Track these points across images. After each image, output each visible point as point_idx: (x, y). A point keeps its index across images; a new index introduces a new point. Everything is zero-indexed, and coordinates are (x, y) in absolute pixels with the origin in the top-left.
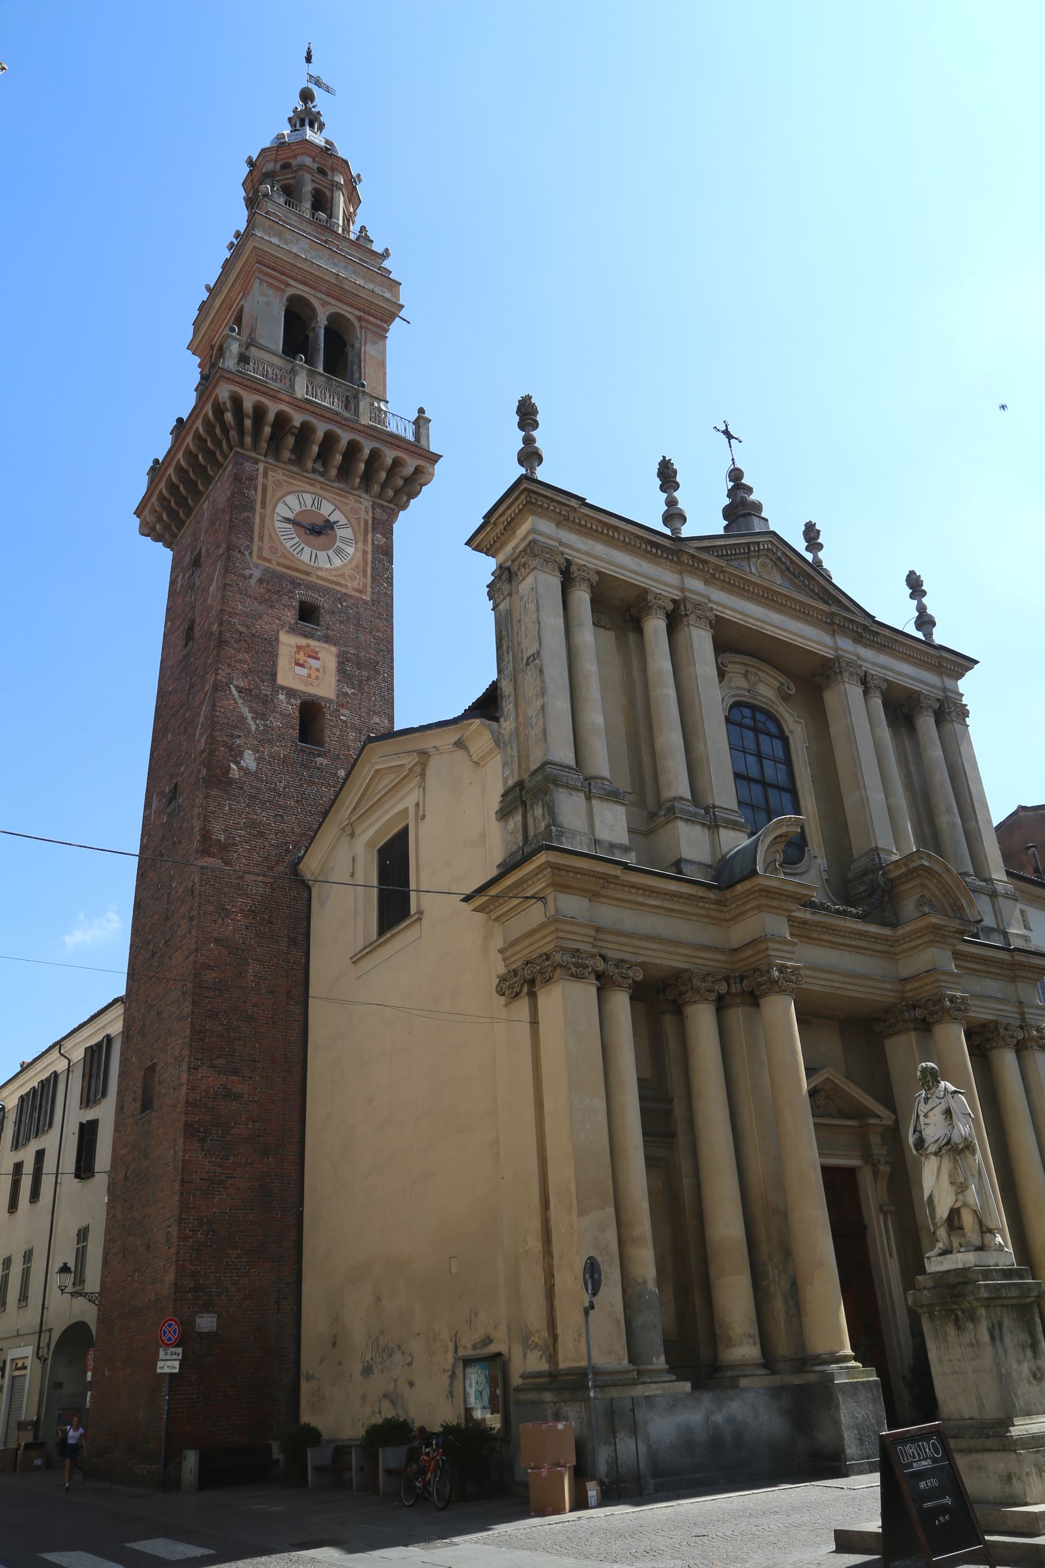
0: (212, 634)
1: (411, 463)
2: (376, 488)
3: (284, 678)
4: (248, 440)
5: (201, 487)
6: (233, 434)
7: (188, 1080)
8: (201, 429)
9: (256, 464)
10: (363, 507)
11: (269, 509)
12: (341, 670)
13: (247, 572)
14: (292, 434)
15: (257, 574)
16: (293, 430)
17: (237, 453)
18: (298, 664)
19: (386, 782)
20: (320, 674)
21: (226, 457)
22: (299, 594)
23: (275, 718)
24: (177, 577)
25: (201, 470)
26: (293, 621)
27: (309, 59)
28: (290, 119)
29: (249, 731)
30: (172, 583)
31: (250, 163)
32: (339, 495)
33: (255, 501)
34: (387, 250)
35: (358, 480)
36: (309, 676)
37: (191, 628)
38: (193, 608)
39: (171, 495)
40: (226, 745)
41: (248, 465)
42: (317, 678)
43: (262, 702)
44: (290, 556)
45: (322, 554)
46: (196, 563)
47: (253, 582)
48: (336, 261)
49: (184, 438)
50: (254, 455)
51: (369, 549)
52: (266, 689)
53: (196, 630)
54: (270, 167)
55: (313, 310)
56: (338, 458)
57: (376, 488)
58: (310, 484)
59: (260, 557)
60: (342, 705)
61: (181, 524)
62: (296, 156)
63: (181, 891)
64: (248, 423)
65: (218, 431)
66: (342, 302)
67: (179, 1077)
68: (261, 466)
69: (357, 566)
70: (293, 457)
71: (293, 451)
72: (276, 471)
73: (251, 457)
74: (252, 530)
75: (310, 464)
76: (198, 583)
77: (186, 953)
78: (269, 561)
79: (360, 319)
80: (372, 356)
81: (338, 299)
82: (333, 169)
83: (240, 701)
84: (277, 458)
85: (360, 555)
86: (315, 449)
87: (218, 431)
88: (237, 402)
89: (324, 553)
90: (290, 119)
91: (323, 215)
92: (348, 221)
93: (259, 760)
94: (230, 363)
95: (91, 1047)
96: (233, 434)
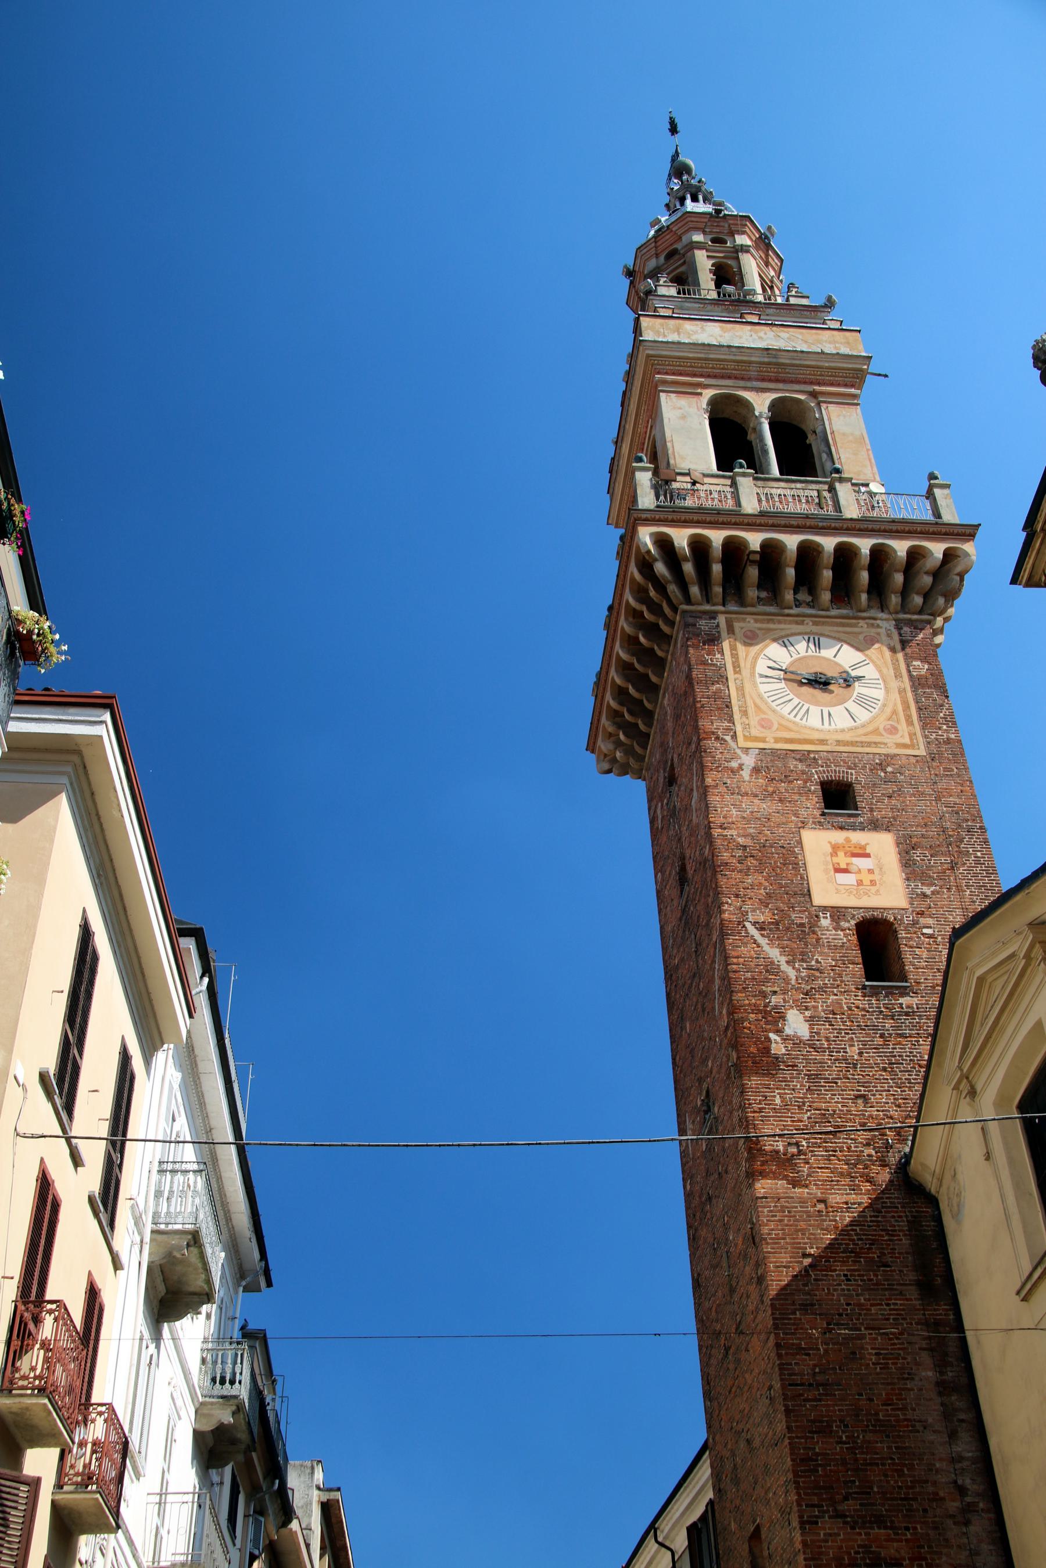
0: (706, 860)
1: (937, 549)
2: (894, 600)
4: (695, 590)
5: (654, 679)
6: (672, 588)
7: (804, 1543)
8: (631, 601)
9: (714, 618)
10: (882, 631)
11: (746, 673)
12: (907, 864)
13: (734, 764)
14: (753, 562)
15: (749, 761)
16: (752, 557)
17: (684, 612)
18: (838, 870)
19: (999, 990)
20: (876, 877)
21: (672, 624)
23: (821, 954)
24: (655, 812)
25: (646, 655)
26: (817, 813)
27: (674, 129)
28: (667, 206)
29: (787, 980)
30: (653, 821)
31: (630, 273)
32: (843, 625)
34: (829, 299)
35: (864, 597)
36: (860, 883)
37: (683, 869)
38: (680, 839)
39: (621, 704)
40: (756, 1010)
41: (703, 624)
42: (873, 883)
44: (791, 725)
45: (838, 711)
46: (671, 780)
47: (746, 774)
48: (762, 334)
49: (617, 622)
50: (707, 607)
51: (907, 684)
53: (688, 867)
54: (652, 264)
55: (748, 406)
56: (827, 575)
57: (894, 600)
58: (797, 623)
59: (746, 738)
60: (921, 914)
61: (644, 739)
62: (680, 238)
63: (740, 1242)
64: (688, 568)
65: (652, 593)
66: (784, 381)
67: (791, 1540)
68: (722, 619)
69: (894, 712)
70: (764, 594)
71: (760, 587)
72: (744, 620)
73: (705, 612)
74: (729, 706)
75: (789, 596)
76: (678, 805)
77: (763, 1337)
79: (814, 395)
80: (844, 434)
81: (777, 380)
82: (732, 234)
83: (763, 942)
84: (742, 602)
85: (896, 696)
86: (791, 572)
87: (652, 593)
88: (664, 544)
89: (841, 708)
90: (667, 206)
91: (730, 289)
92: (771, 288)
93: (810, 1020)
94: (646, 499)
95: (694, 1524)
96: (672, 588)
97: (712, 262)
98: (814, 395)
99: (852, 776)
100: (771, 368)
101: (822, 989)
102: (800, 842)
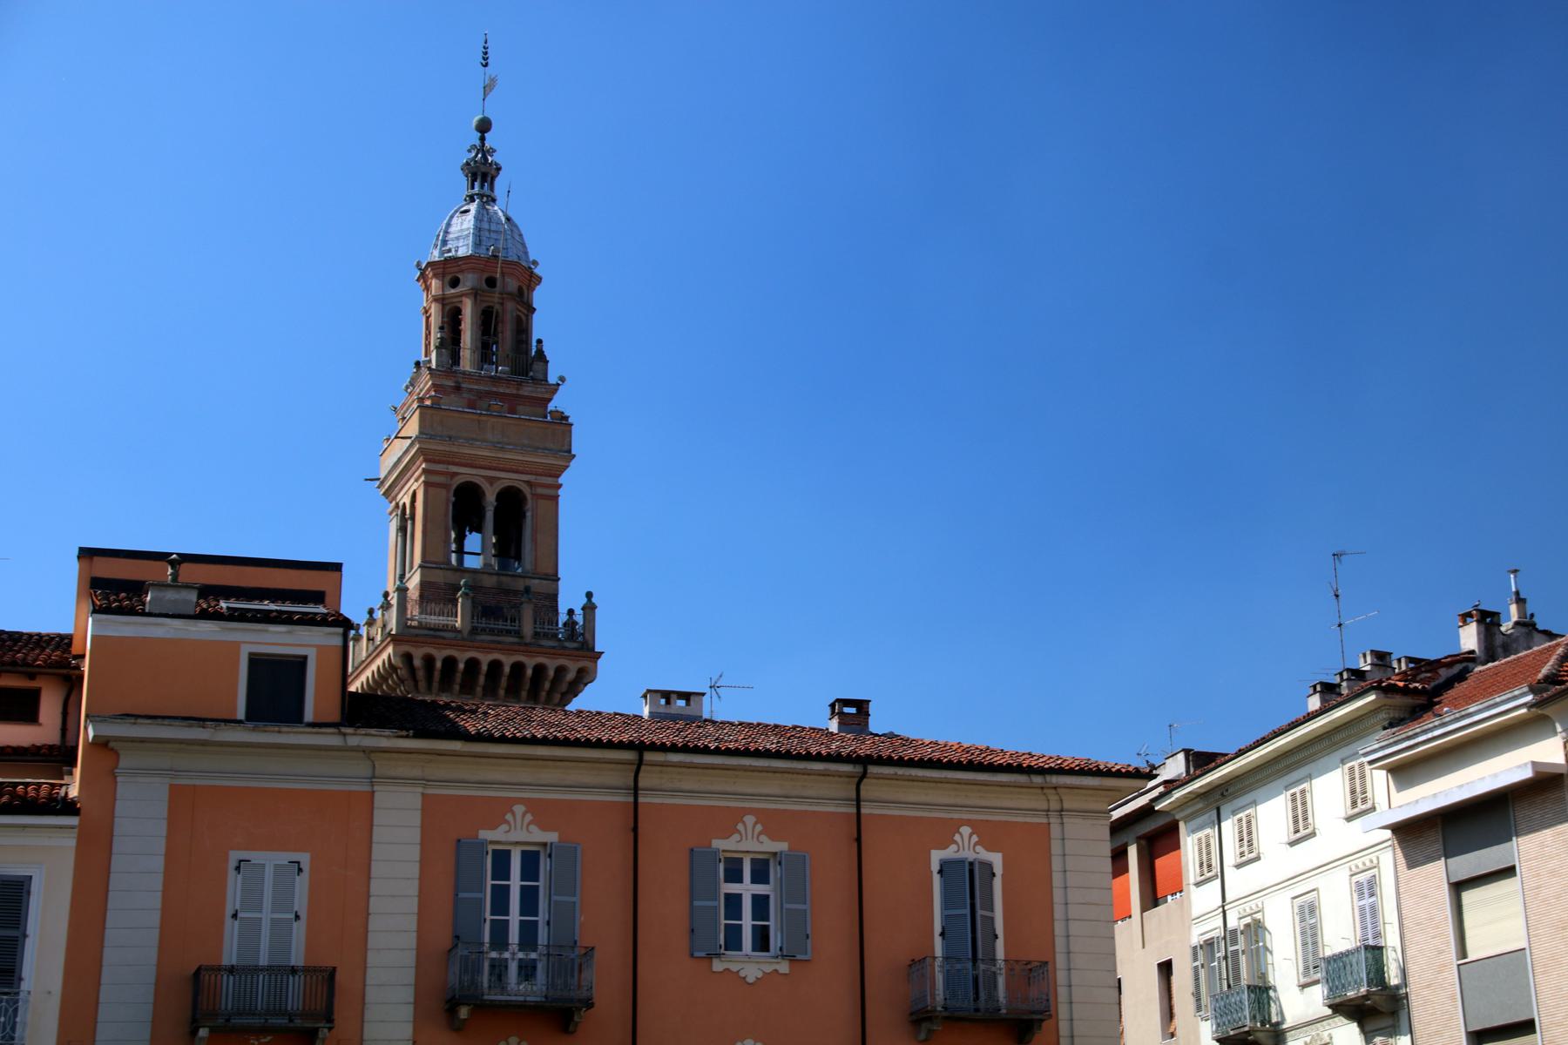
1: (573, 667)
4: (422, 685)
64: (421, 674)
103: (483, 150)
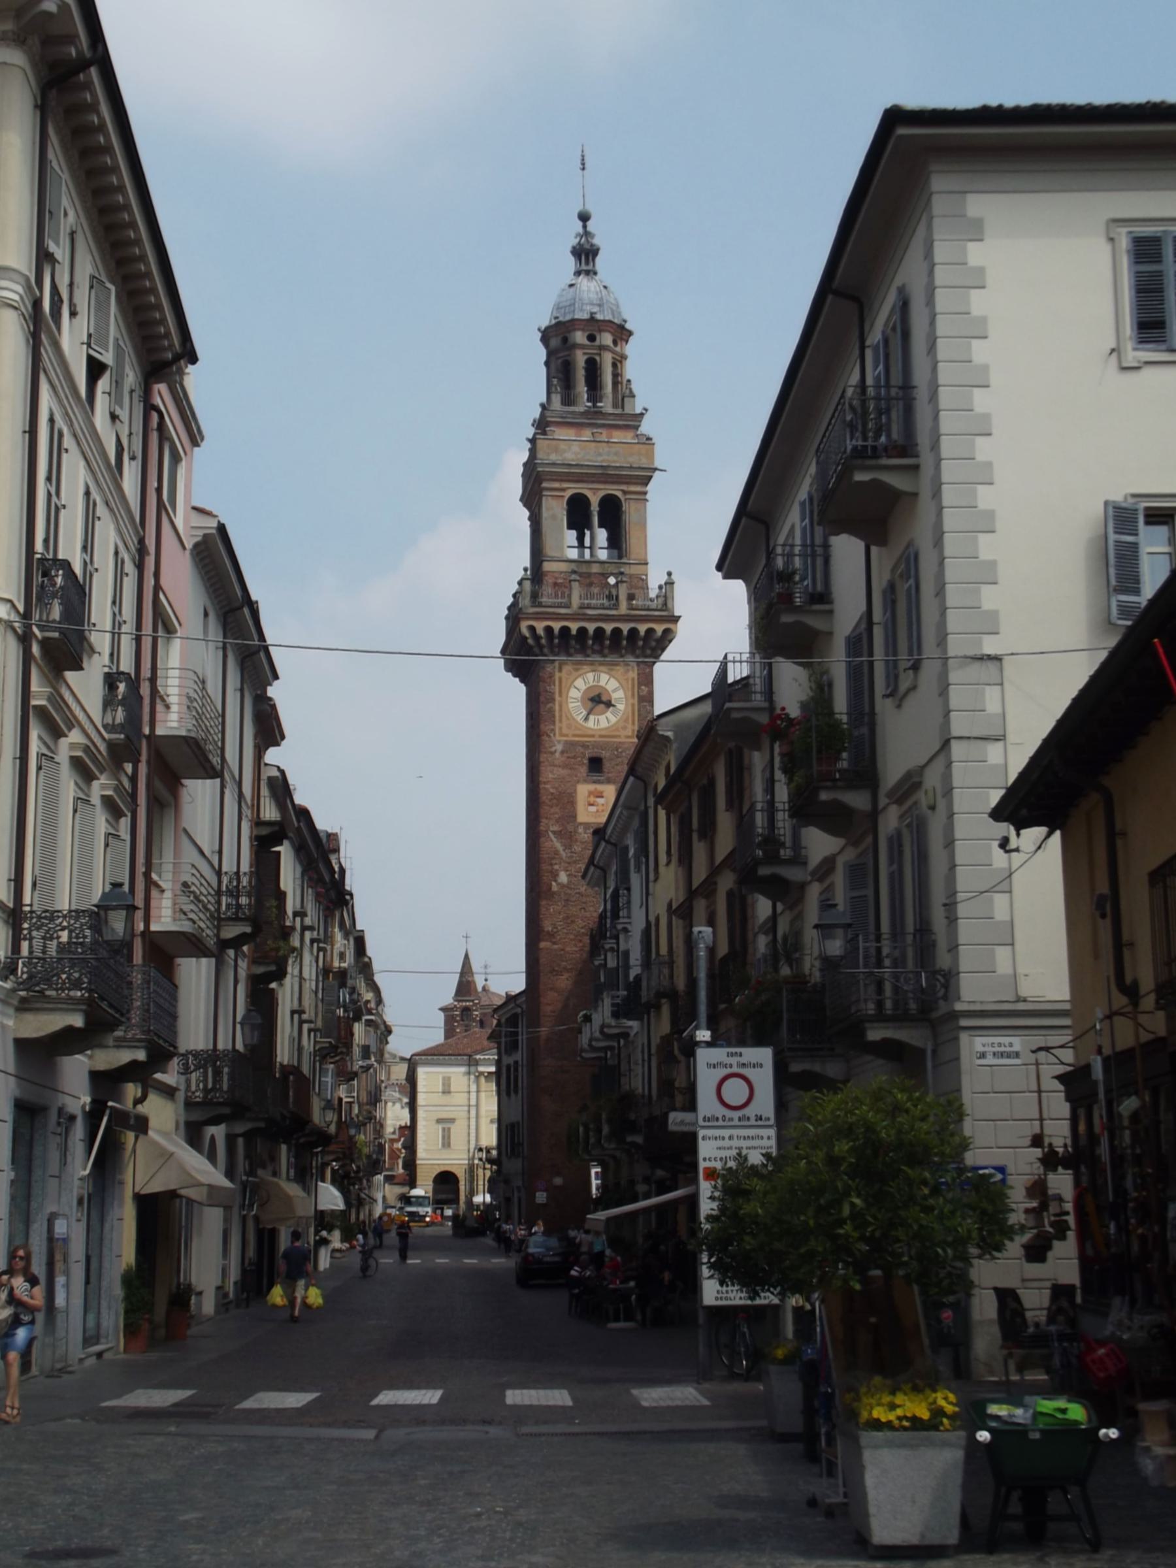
1: (659, 628)
3: (582, 818)
13: (553, 749)
15: (559, 747)
22: (588, 753)
33: (553, 693)
43: (568, 837)
47: (557, 755)
52: (570, 828)
59: (562, 735)
64: (543, 641)
68: (557, 664)
78: (567, 735)
79: (625, 492)
83: (554, 840)
88: (532, 629)
93: (568, 876)
97: (586, 357)
98: (625, 492)
99: (604, 754)
100: (604, 475)
101: (575, 862)
102: (575, 791)
103: (587, 234)
